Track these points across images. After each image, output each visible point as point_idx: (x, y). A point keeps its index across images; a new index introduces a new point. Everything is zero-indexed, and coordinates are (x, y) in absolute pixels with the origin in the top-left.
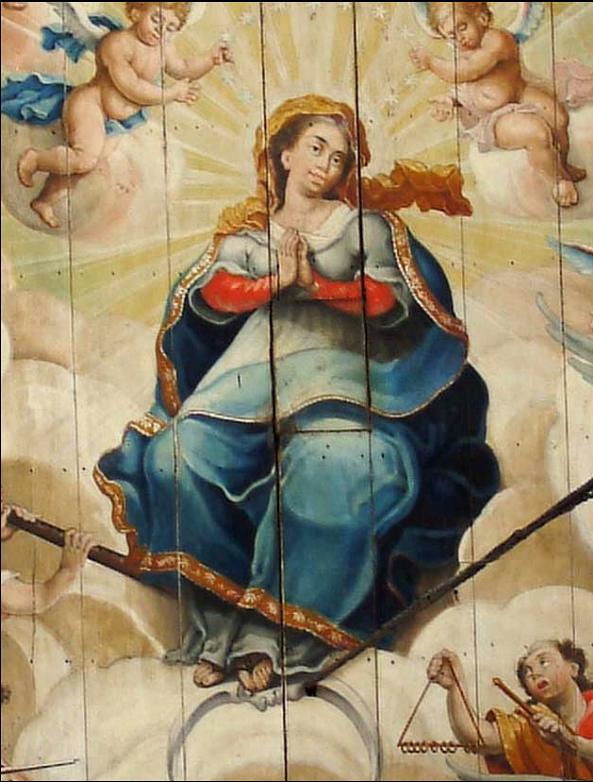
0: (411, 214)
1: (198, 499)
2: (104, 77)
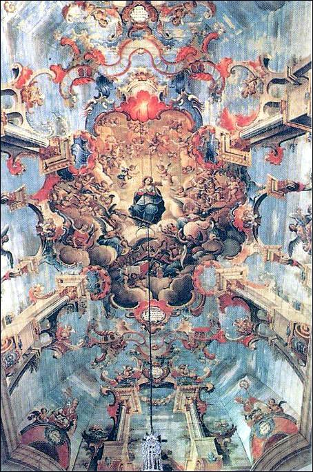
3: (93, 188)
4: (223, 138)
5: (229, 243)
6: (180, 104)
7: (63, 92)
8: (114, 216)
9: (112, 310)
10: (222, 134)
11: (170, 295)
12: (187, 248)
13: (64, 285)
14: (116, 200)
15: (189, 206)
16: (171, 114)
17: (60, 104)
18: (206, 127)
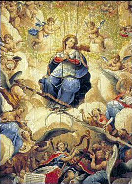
8: (18, 90)
12: (119, 150)
14: (22, 66)
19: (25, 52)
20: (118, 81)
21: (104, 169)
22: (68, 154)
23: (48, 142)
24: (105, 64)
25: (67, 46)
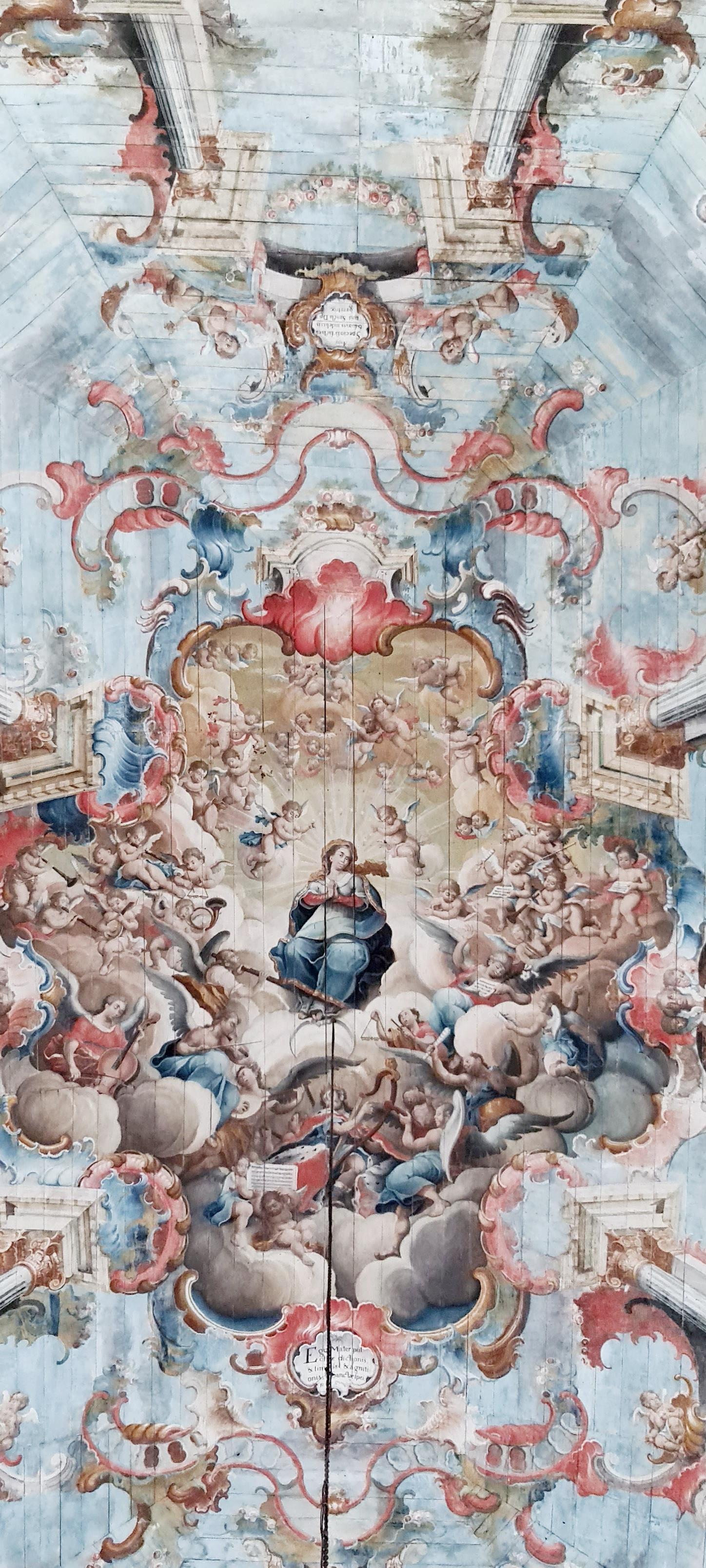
0: (370, 876)
1: (302, 964)
2: (274, 831)
3: (155, 870)
4: (592, 729)
5: (611, 1087)
6: (455, 610)
7: (82, 550)
8: (220, 975)
9: (185, 1336)
10: (590, 709)
11: (399, 1287)
12: (467, 1103)
13: (19, 1224)
14: (227, 919)
15: (479, 949)
16: (425, 638)
17: (70, 583)
18: (538, 684)
19: (233, 887)
20: (456, 942)
21: (434, 1147)
22: (347, 1115)
23: (300, 1091)
24: (425, 902)
25: (333, 868)
